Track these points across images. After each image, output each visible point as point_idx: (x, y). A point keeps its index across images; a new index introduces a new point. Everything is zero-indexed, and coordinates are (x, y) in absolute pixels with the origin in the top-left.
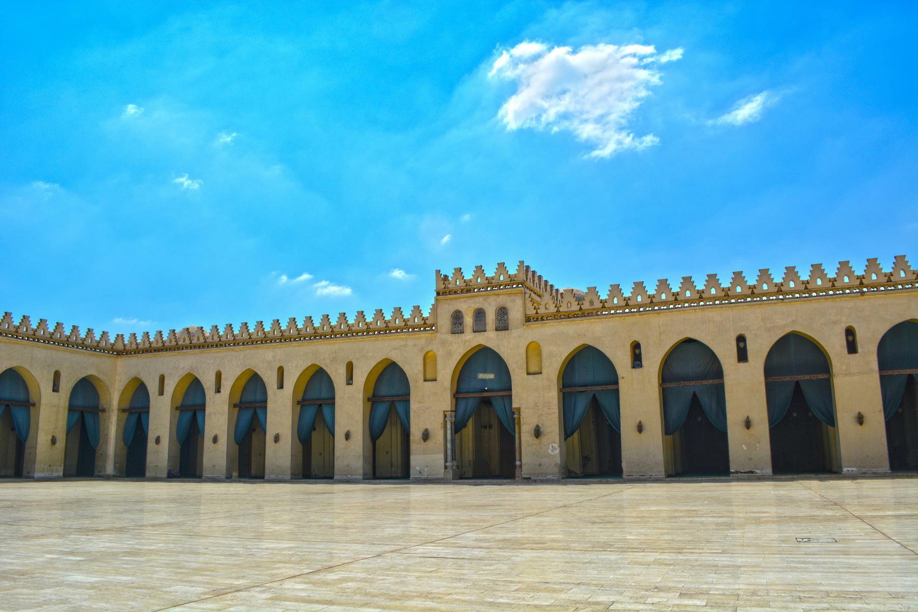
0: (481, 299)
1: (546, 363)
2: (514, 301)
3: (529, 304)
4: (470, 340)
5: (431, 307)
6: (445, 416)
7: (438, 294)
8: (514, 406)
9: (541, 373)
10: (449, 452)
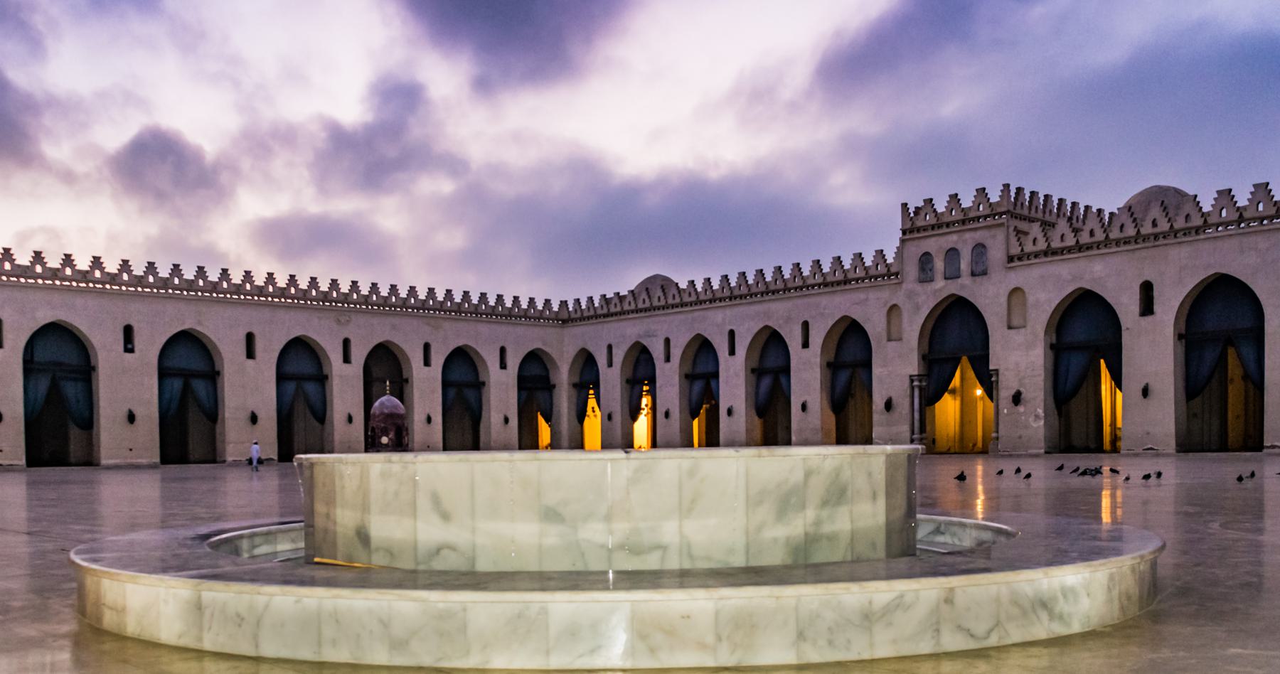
0: (954, 237)
1: (1032, 314)
2: (994, 237)
3: (1013, 240)
4: (941, 288)
5: (896, 250)
6: (912, 381)
7: (904, 232)
8: (991, 367)
9: (1024, 327)
10: (917, 424)
